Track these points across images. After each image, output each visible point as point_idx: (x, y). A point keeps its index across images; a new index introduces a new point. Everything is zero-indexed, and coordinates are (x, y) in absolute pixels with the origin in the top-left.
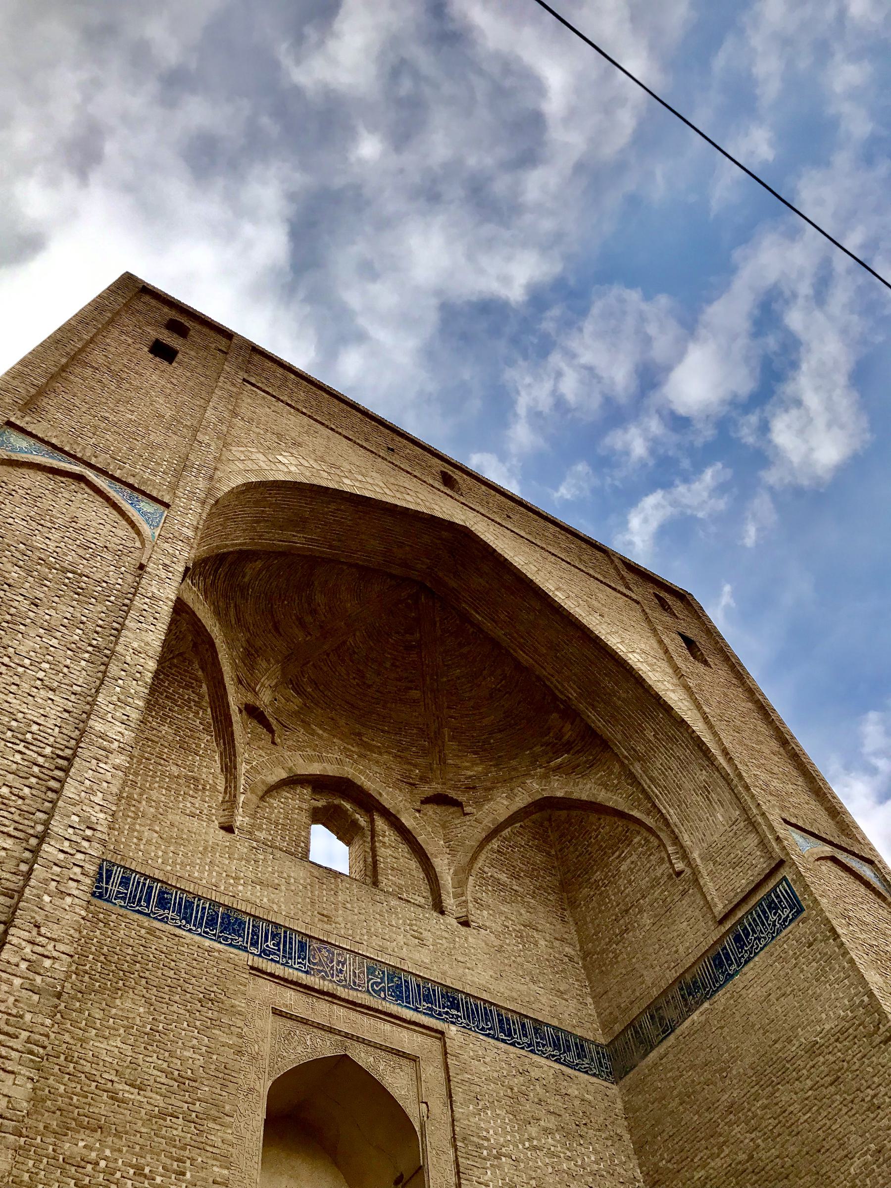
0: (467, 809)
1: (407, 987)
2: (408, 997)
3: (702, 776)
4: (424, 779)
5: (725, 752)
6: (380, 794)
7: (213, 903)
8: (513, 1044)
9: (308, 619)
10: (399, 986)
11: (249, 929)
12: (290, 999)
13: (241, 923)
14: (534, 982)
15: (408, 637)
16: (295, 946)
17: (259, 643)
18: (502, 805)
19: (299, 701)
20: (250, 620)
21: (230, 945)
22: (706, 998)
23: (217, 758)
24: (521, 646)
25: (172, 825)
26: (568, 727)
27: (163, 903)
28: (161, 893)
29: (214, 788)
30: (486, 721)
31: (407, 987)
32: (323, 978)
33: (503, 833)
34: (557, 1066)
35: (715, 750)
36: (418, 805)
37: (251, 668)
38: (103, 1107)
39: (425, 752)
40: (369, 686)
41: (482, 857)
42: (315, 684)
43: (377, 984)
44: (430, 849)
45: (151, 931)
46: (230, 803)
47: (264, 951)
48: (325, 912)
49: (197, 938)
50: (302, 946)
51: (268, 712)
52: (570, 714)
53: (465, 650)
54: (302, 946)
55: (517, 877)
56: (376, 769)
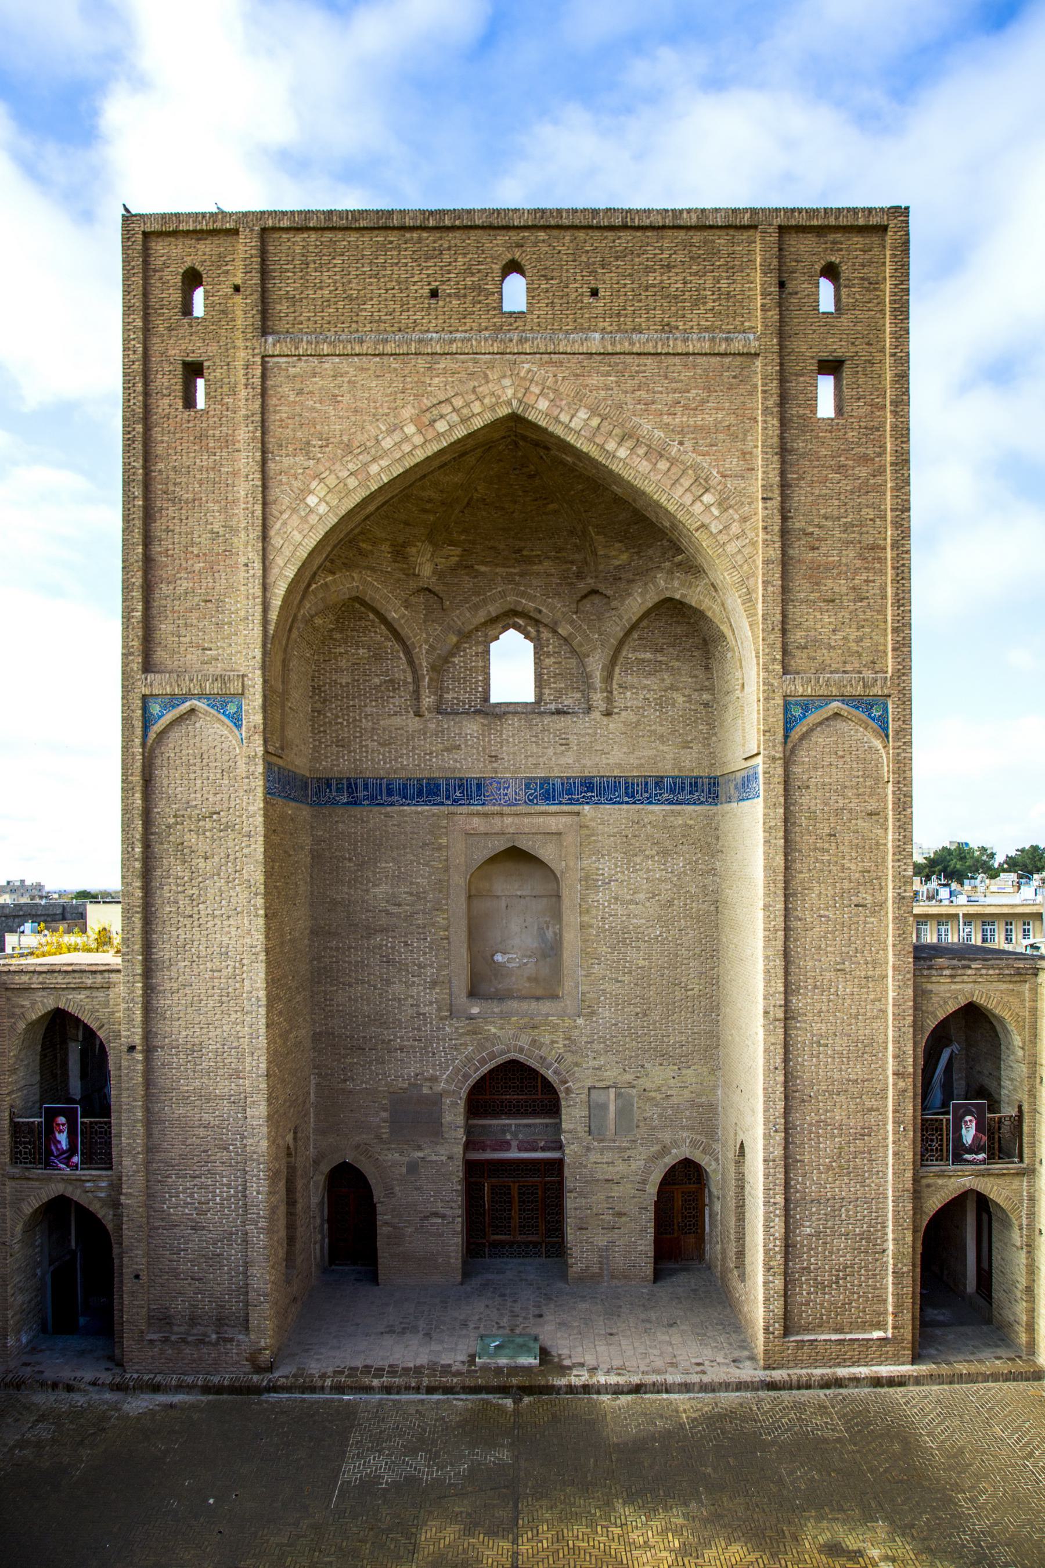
1: (554, 789)
2: (554, 796)
4: (580, 576)
6: (540, 611)
7: (419, 780)
8: (634, 803)
10: (547, 791)
11: (443, 788)
13: (438, 786)
14: (663, 743)
16: (474, 788)
19: (458, 551)
21: (434, 804)
23: (402, 655)
25: (384, 729)
27: (390, 793)
28: (388, 785)
29: (406, 683)
31: (554, 789)
32: (494, 805)
33: (641, 626)
34: (668, 807)
36: (574, 606)
38: (384, 921)
39: (578, 549)
40: (513, 513)
41: (626, 647)
43: (531, 795)
45: (387, 815)
47: (454, 801)
48: (493, 754)
49: (413, 808)
50: (479, 786)
54: (479, 786)
55: (662, 650)
56: (535, 582)
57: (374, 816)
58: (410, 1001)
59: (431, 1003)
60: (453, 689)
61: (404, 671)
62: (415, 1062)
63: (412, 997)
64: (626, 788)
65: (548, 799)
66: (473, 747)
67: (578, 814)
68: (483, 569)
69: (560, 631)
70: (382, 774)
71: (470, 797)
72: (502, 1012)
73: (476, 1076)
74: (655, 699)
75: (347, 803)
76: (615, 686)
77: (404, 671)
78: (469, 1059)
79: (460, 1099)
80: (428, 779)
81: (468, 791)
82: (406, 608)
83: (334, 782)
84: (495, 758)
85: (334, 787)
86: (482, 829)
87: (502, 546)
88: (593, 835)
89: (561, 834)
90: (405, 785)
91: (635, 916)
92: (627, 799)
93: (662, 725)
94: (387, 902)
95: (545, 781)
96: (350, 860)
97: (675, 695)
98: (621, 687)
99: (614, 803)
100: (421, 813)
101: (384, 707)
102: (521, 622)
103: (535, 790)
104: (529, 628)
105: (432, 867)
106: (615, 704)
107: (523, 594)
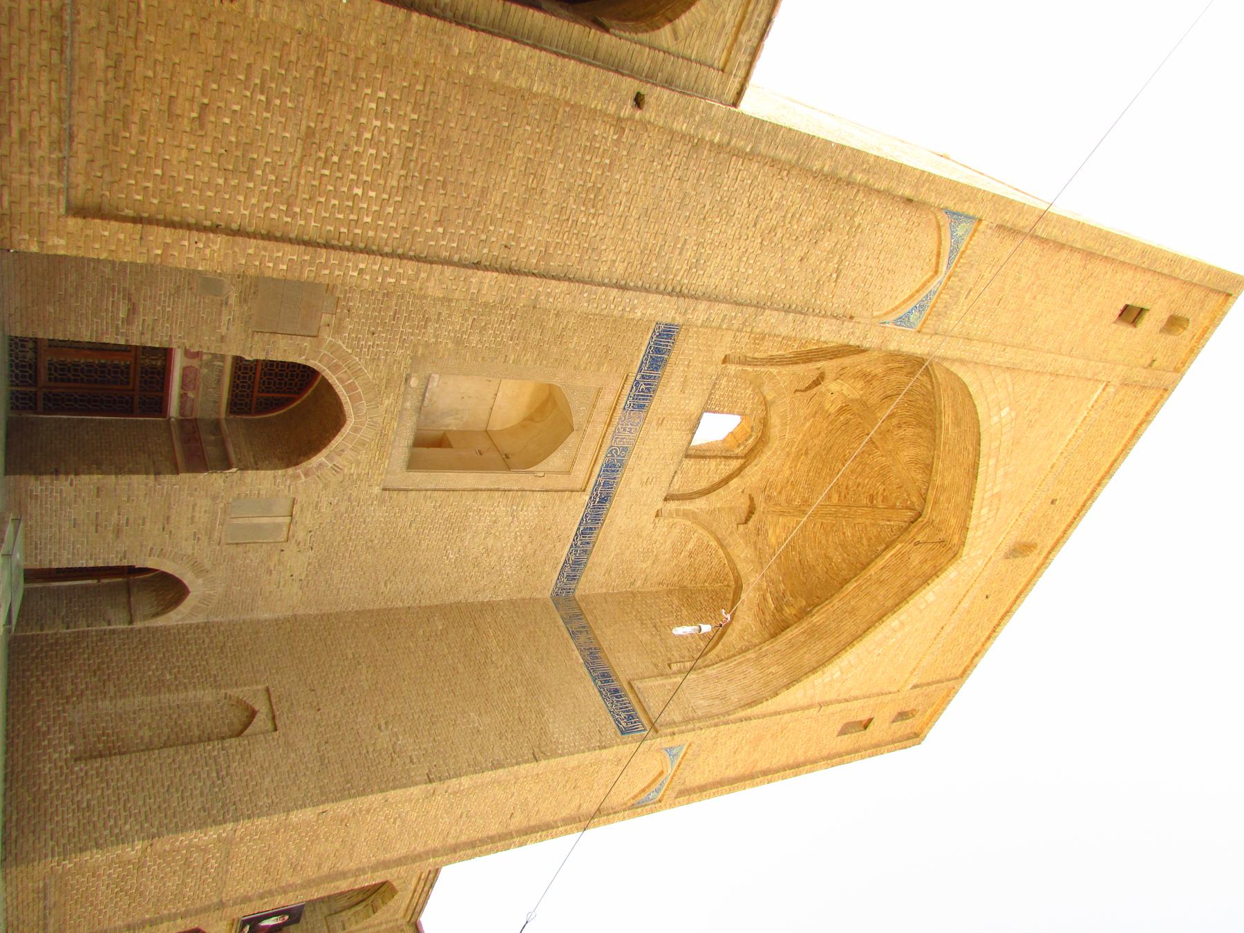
0: (741, 527)
3: (734, 698)
4: (769, 498)
5: (748, 719)
9: (895, 421)
11: (654, 374)
15: (880, 499)
16: (641, 402)
17: (875, 383)
18: (742, 553)
19: (833, 410)
20: (892, 377)
22: (586, 662)
24: (859, 587)
26: (794, 612)
29: (756, 350)
30: (808, 550)
35: (749, 712)
37: (855, 377)
39: (789, 501)
41: (705, 533)
42: (847, 422)
44: (713, 496)
46: (744, 361)
51: (821, 388)
52: (803, 614)
53: (865, 541)
56: (778, 463)
58: (445, 312)
59: (436, 337)
62: (367, 309)
63: (450, 316)
68: (808, 424)
72: (406, 409)
78: (357, 373)
79: (307, 360)
84: (660, 423)
87: (816, 441)
95: (622, 464)
97: (649, 562)
100: (639, 350)
102: (750, 441)
105: (584, 355)
107: (775, 453)
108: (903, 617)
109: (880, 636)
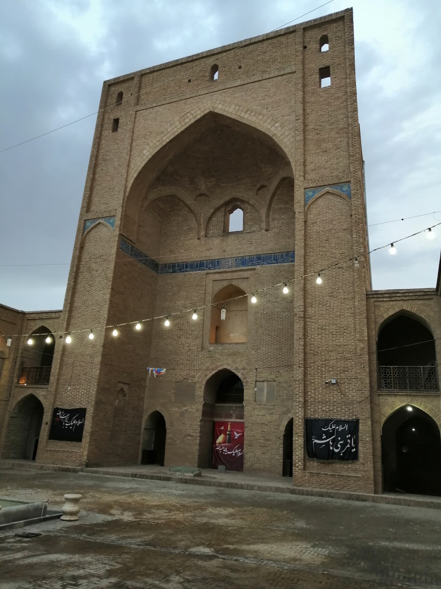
6: (243, 197)
7: (197, 262)
8: (277, 263)
11: (205, 264)
12: (217, 277)
14: (289, 239)
27: (186, 267)
32: (223, 268)
41: (273, 203)
45: (185, 275)
47: (209, 268)
49: (194, 272)
50: (218, 262)
57: (180, 276)
60: (212, 229)
61: (195, 224)
64: (274, 257)
65: (243, 264)
66: (217, 248)
67: (254, 269)
68: (224, 185)
69: (251, 203)
70: (184, 261)
71: (215, 266)
73: (210, 375)
74: (286, 222)
75: (172, 272)
76: (270, 219)
77: (195, 224)
80: (200, 261)
81: (214, 264)
82: (195, 200)
83: (168, 265)
85: (167, 267)
86: (219, 278)
88: (260, 277)
89: (248, 278)
90: (192, 264)
91: (277, 308)
92: (274, 262)
93: (289, 232)
94: (182, 307)
96: (170, 292)
98: (273, 220)
99: (269, 264)
101: (187, 237)
103: (239, 261)
104: (242, 205)
106: (270, 226)
108: (242, 114)
109: (254, 119)
